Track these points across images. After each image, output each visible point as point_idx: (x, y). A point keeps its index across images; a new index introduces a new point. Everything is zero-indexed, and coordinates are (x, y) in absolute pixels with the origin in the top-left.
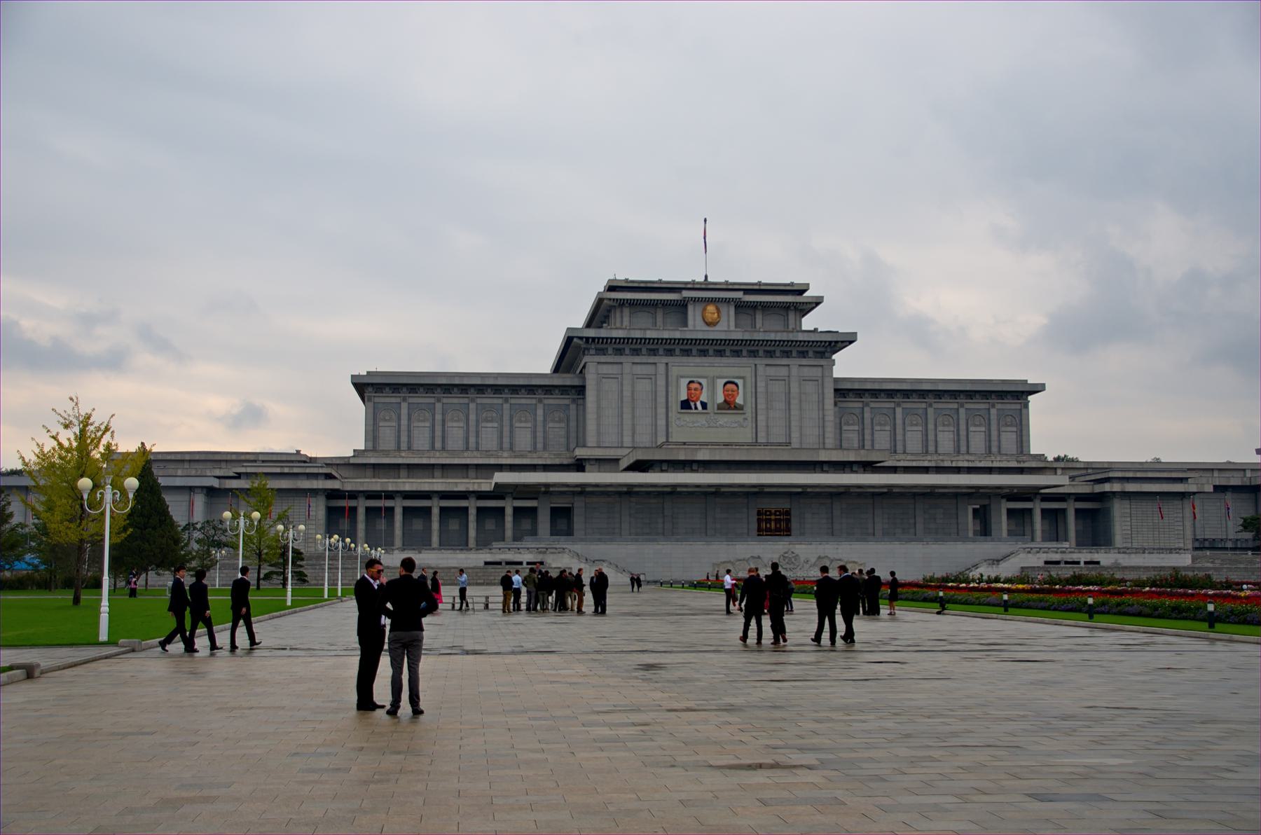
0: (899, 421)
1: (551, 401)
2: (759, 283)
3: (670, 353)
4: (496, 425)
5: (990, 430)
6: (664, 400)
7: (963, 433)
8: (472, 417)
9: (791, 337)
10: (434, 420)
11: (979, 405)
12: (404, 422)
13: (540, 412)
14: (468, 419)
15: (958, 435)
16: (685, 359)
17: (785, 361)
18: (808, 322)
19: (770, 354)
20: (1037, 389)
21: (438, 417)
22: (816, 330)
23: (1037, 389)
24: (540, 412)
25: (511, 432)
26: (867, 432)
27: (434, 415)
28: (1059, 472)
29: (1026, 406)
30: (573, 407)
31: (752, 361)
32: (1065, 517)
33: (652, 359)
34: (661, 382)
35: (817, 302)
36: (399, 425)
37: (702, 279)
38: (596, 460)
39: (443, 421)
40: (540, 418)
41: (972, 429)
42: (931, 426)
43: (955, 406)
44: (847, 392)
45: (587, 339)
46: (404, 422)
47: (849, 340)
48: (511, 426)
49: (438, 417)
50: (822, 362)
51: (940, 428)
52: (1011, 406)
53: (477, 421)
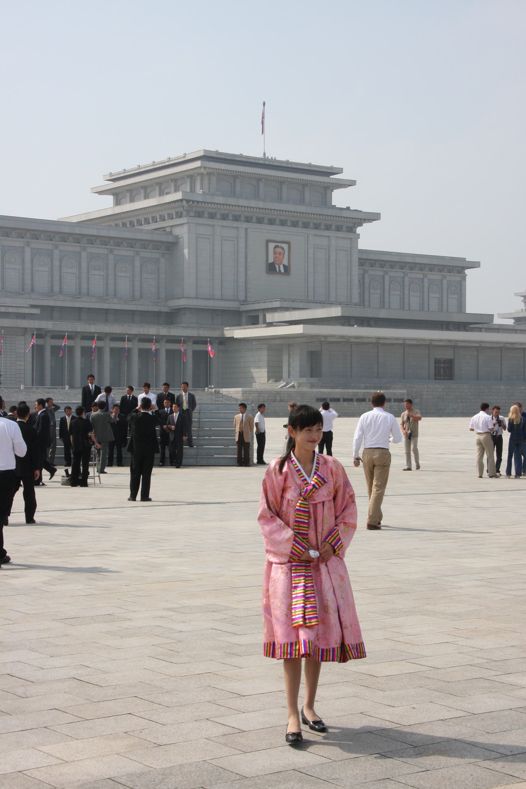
0: (387, 287)
1: (147, 254)
2: (310, 165)
3: (248, 220)
4: (102, 273)
5: (442, 297)
6: (244, 260)
7: (426, 298)
8: (84, 265)
9: (326, 211)
10: (52, 264)
11: (435, 276)
12: (28, 265)
13: (137, 264)
14: (80, 267)
15: (423, 299)
16: (259, 226)
17: (327, 233)
18: (340, 198)
19: (317, 227)
20: (475, 265)
21: (56, 263)
22: (348, 208)
23: (475, 265)
24: (137, 264)
25: (115, 279)
26: (366, 294)
27: (52, 260)
28: (483, 330)
29: (464, 278)
30: (162, 260)
31: (305, 230)
32: (129, 358)
33: (235, 224)
34: (242, 244)
35: (352, 183)
36: (23, 269)
37: (261, 156)
38: (197, 309)
39: (60, 267)
40: (137, 269)
41: (431, 295)
42: (406, 292)
43: (421, 276)
44: (373, 262)
45: (193, 202)
46: (28, 265)
47: (373, 217)
48: (115, 274)
49: (56, 263)
50: (351, 235)
51: (411, 294)
52: (454, 278)
53: (88, 269)
